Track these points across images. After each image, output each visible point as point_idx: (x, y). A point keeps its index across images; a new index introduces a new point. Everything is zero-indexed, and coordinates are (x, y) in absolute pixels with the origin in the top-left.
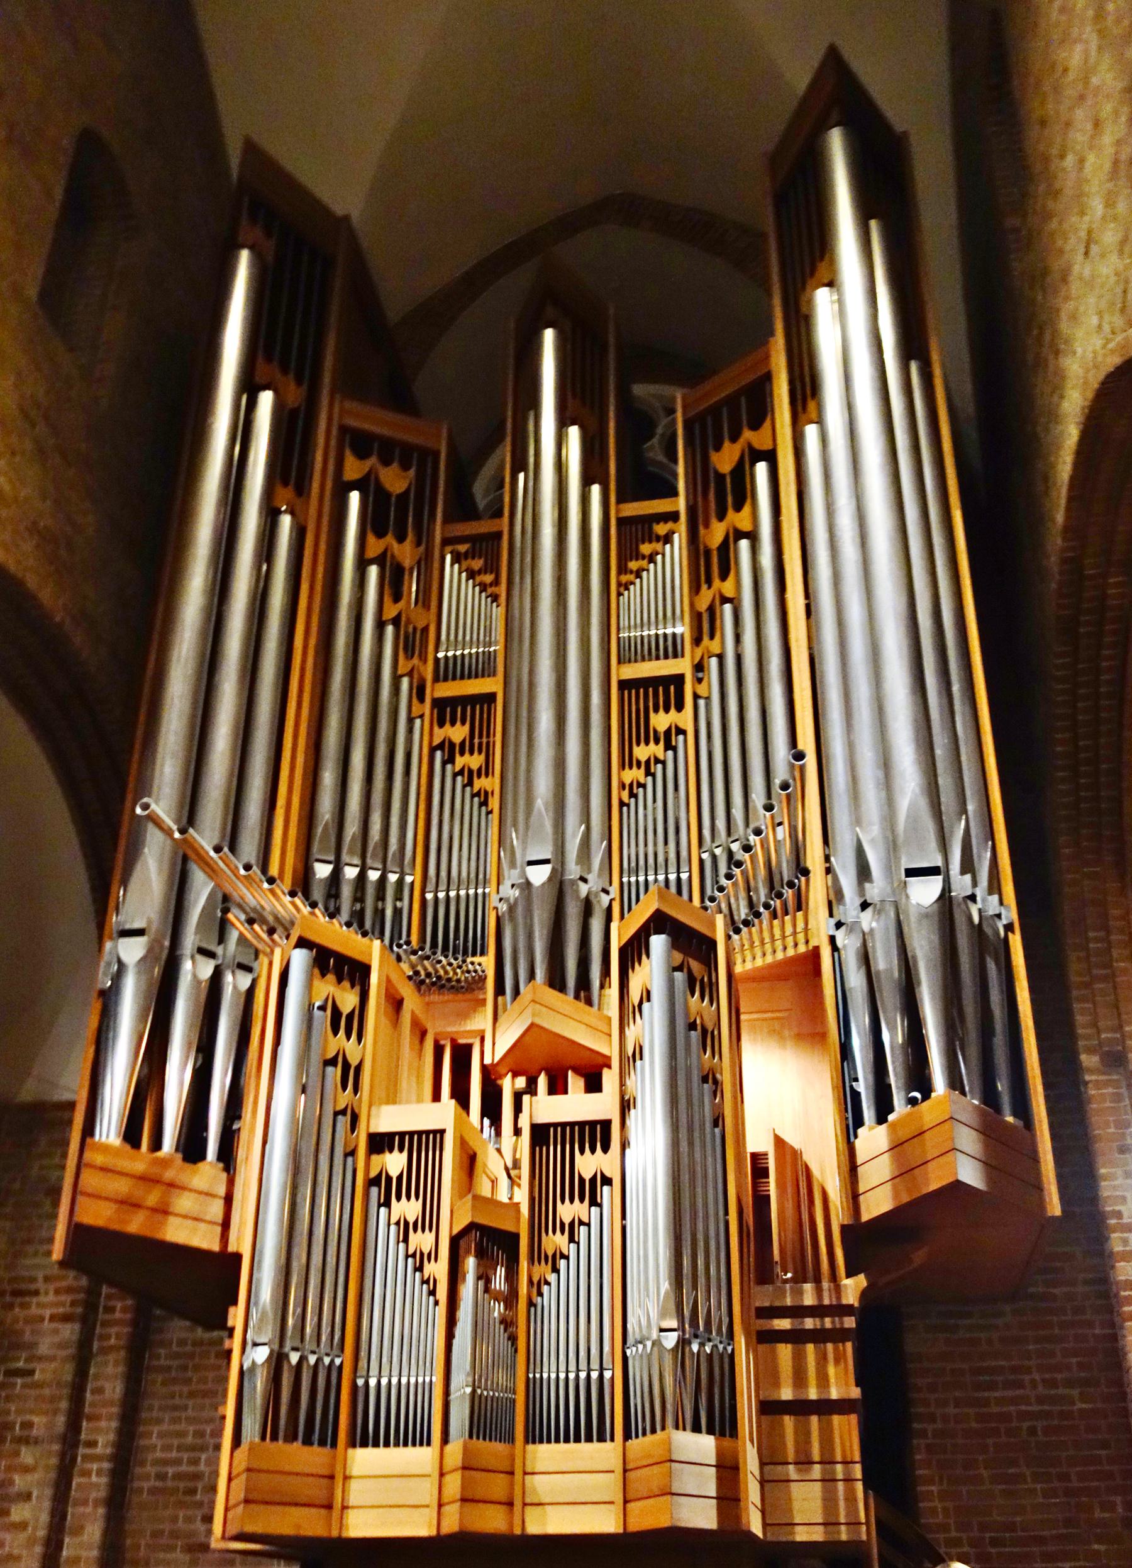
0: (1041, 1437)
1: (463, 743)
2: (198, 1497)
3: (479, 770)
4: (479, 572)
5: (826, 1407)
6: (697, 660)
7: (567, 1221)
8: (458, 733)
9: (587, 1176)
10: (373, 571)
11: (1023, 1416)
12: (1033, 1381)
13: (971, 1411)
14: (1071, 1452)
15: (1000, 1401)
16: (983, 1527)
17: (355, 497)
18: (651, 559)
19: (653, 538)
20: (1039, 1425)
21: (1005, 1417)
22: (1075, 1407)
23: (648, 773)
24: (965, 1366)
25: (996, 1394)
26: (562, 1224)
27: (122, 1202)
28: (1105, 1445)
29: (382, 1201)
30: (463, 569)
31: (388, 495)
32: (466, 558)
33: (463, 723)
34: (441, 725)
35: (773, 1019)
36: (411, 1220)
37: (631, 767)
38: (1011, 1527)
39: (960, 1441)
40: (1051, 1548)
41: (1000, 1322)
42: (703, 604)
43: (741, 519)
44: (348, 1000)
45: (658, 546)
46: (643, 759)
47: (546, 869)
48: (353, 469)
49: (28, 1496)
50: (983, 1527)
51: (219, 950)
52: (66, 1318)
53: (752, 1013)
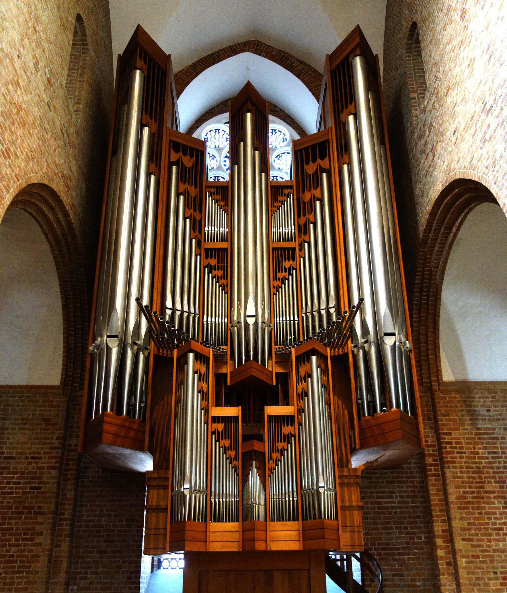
0: (398, 515)
1: (215, 266)
2: (102, 533)
3: (222, 276)
4: (219, 201)
5: (351, 508)
6: (300, 242)
7: (280, 449)
8: (213, 262)
9: (286, 433)
11: (393, 508)
12: (396, 497)
13: (376, 506)
14: (408, 520)
15: (385, 503)
16: (379, 544)
18: (283, 203)
19: (282, 194)
20: (398, 510)
21: (387, 508)
22: (410, 505)
23: (282, 283)
24: (374, 490)
25: (385, 500)
26: (278, 450)
27: (115, 435)
28: (419, 517)
30: (213, 199)
33: (215, 258)
34: (207, 258)
37: (276, 280)
38: (388, 544)
39: (372, 516)
40: (401, 551)
41: (386, 476)
42: (302, 223)
46: (281, 277)
47: (253, 319)
49: (41, 534)
50: (379, 544)
51: (149, 347)
52: (53, 468)
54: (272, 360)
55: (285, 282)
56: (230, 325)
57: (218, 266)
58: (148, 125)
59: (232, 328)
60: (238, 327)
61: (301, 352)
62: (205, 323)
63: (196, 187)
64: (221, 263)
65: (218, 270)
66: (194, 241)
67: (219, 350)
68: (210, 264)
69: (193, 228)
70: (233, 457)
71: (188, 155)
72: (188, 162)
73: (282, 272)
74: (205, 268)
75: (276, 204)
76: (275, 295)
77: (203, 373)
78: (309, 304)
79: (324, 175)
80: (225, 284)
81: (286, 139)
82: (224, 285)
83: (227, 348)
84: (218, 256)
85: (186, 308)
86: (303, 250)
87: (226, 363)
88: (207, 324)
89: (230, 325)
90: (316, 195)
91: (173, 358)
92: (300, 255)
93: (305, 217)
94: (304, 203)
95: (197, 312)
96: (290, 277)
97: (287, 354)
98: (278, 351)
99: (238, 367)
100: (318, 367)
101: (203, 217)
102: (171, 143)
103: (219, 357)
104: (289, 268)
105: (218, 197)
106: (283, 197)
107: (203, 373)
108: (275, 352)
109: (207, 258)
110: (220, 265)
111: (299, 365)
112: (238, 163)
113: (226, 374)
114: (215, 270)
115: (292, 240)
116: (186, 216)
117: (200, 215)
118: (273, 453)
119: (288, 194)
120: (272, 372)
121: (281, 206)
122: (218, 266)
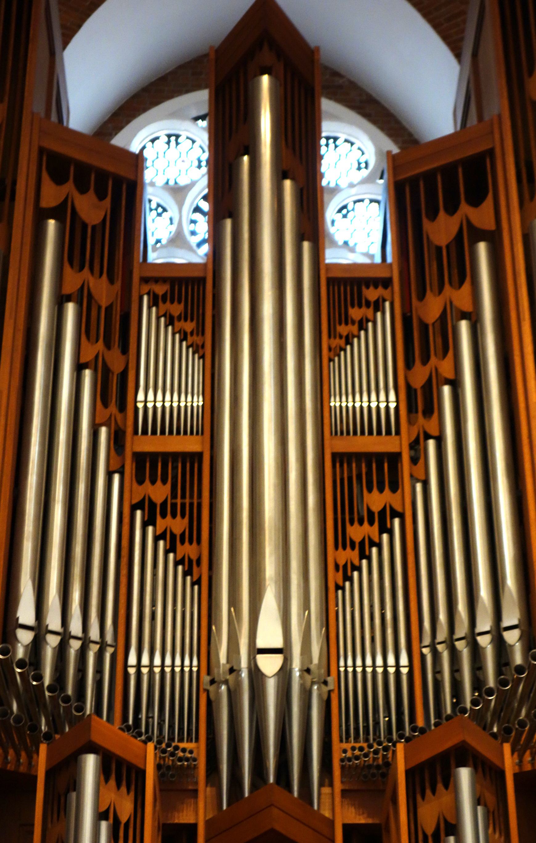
1: (164, 504)
3: (183, 535)
4: (179, 318)
6: (413, 438)
10: (70, 309)
18: (362, 326)
19: (362, 302)
23: (363, 555)
30: (161, 313)
31: (85, 226)
32: (164, 301)
34: (140, 482)
37: (344, 548)
42: (418, 382)
45: (369, 313)
46: (357, 539)
54: (331, 785)
55: (370, 552)
56: (205, 679)
57: (174, 506)
59: (212, 689)
60: (231, 683)
61: (424, 756)
62: (132, 671)
63: (111, 281)
64: (183, 496)
65: (174, 516)
66: (103, 431)
67: (173, 754)
68: (150, 500)
71: (91, 192)
73: (361, 523)
74: (134, 508)
75: (343, 329)
76: (340, 592)
77: (124, 819)
78: (442, 617)
79: (482, 248)
80: (194, 557)
81: (366, 163)
82: (190, 561)
83: (198, 748)
84: (175, 478)
85: (76, 627)
86: (422, 461)
87: (195, 793)
88: (139, 674)
89: (205, 679)
90: (456, 303)
91: (36, 777)
92: (415, 475)
93: (428, 367)
94: (424, 327)
95: (109, 638)
96: (385, 537)
97: (378, 767)
98: (349, 760)
99: (229, 804)
100: (477, 801)
101: (132, 365)
102: (45, 158)
103: (173, 776)
104: (382, 513)
105: (177, 309)
106: (364, 309)
107: (124, 819)
108: (342, 760)
109: (140, 482)
110: (179, 501)
111: (419, 798)
112: (234, 214)
113: (193, 827)
114: (164, 516)
115: (389, 432)
116: (83, 360)
117: (122, 358)
119: (377, 303)
120: (331, 823)
121: (356, 333)
122: (174, 506)
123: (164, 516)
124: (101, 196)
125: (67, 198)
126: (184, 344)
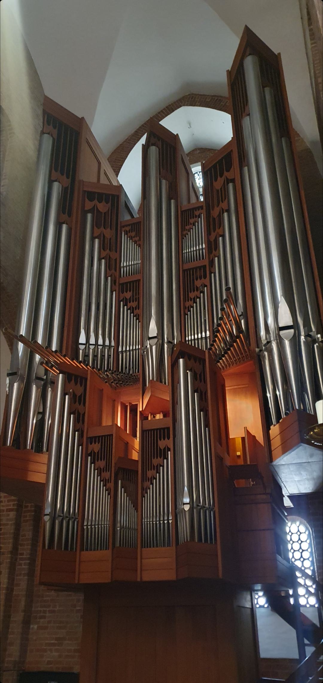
3: (136, 307)
8: (128, 295)
9: (162, 448)
10: (97, 241)
17: (89, 216)
26: (154, 466)
29: (92, 461)
31: (102, 213)
35: (243, 388)
36: (102, 468)
42: (212, 238)
43: (224, 205)
44: (79, 390)
46: (192, 297)
48: (89, 205)
53: (235, 386)
58: (58, 180)
69: (108, 267)
70: (107, 478)
72: (103, 207)
73: (194, 291)
94: (214, 219)
118: (149, 470)
121: (192, 227)
123: (130, 302)
124: (107, 203)
125: (95, 205)
126: (135, 245)
